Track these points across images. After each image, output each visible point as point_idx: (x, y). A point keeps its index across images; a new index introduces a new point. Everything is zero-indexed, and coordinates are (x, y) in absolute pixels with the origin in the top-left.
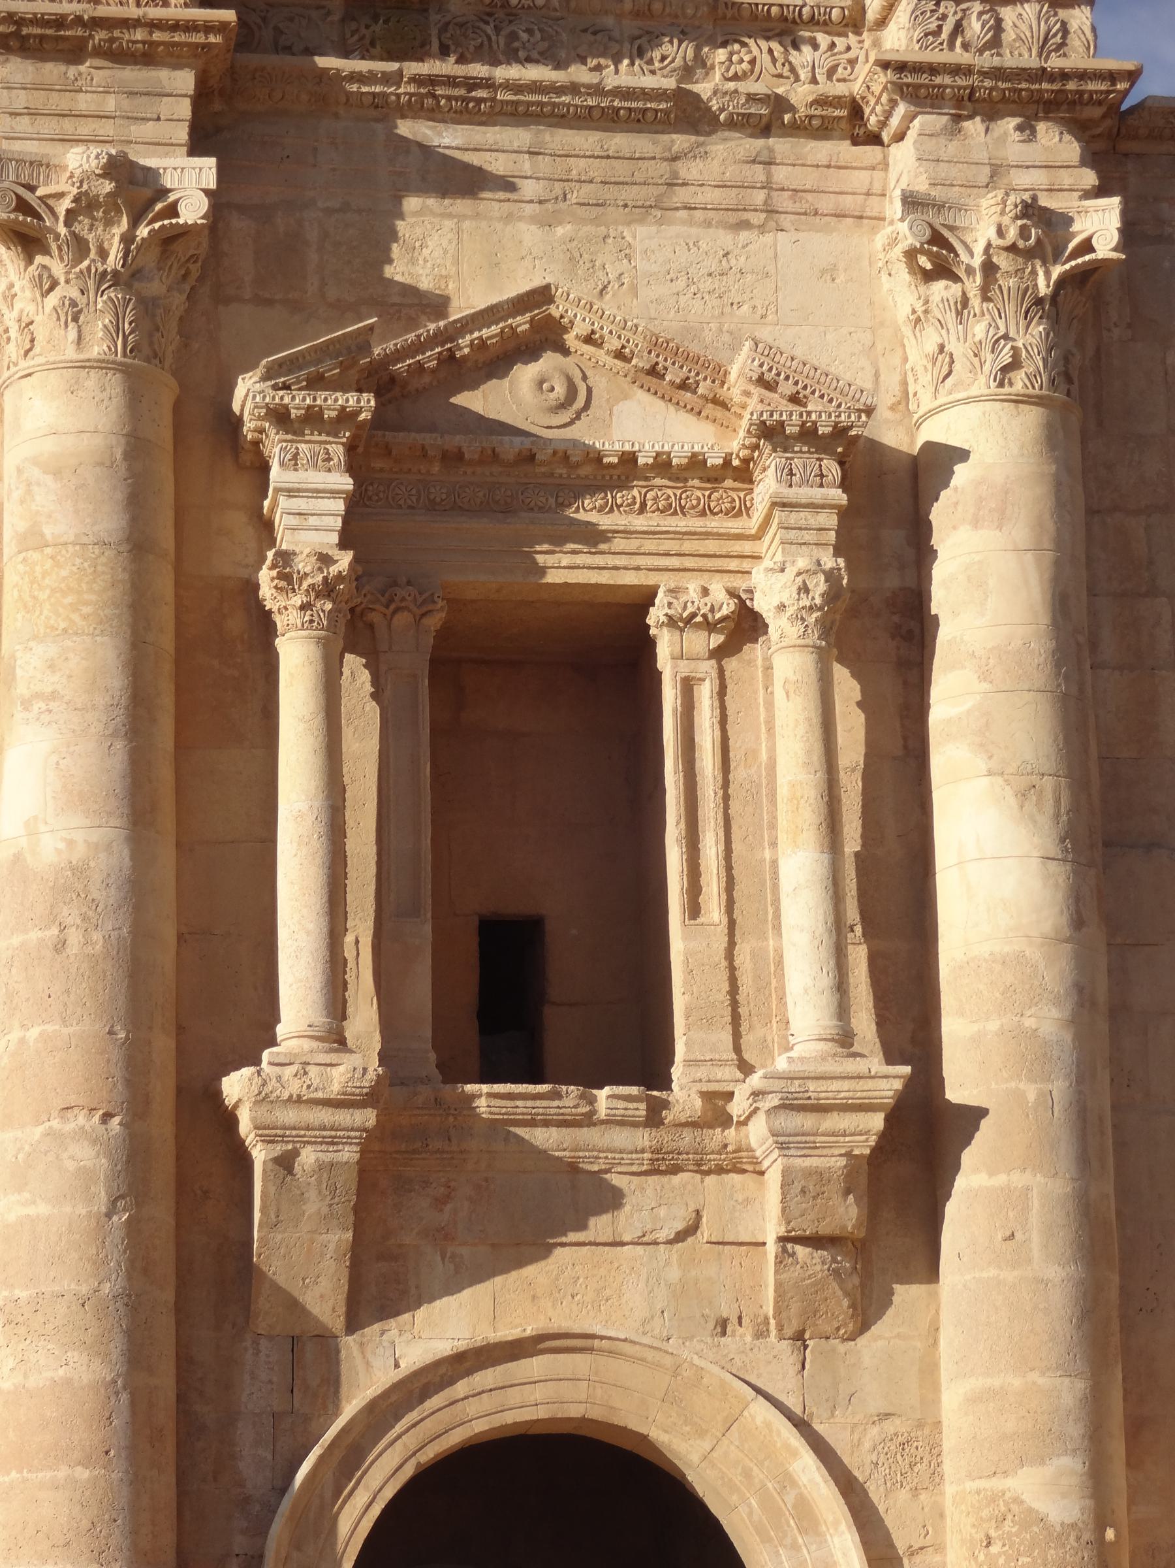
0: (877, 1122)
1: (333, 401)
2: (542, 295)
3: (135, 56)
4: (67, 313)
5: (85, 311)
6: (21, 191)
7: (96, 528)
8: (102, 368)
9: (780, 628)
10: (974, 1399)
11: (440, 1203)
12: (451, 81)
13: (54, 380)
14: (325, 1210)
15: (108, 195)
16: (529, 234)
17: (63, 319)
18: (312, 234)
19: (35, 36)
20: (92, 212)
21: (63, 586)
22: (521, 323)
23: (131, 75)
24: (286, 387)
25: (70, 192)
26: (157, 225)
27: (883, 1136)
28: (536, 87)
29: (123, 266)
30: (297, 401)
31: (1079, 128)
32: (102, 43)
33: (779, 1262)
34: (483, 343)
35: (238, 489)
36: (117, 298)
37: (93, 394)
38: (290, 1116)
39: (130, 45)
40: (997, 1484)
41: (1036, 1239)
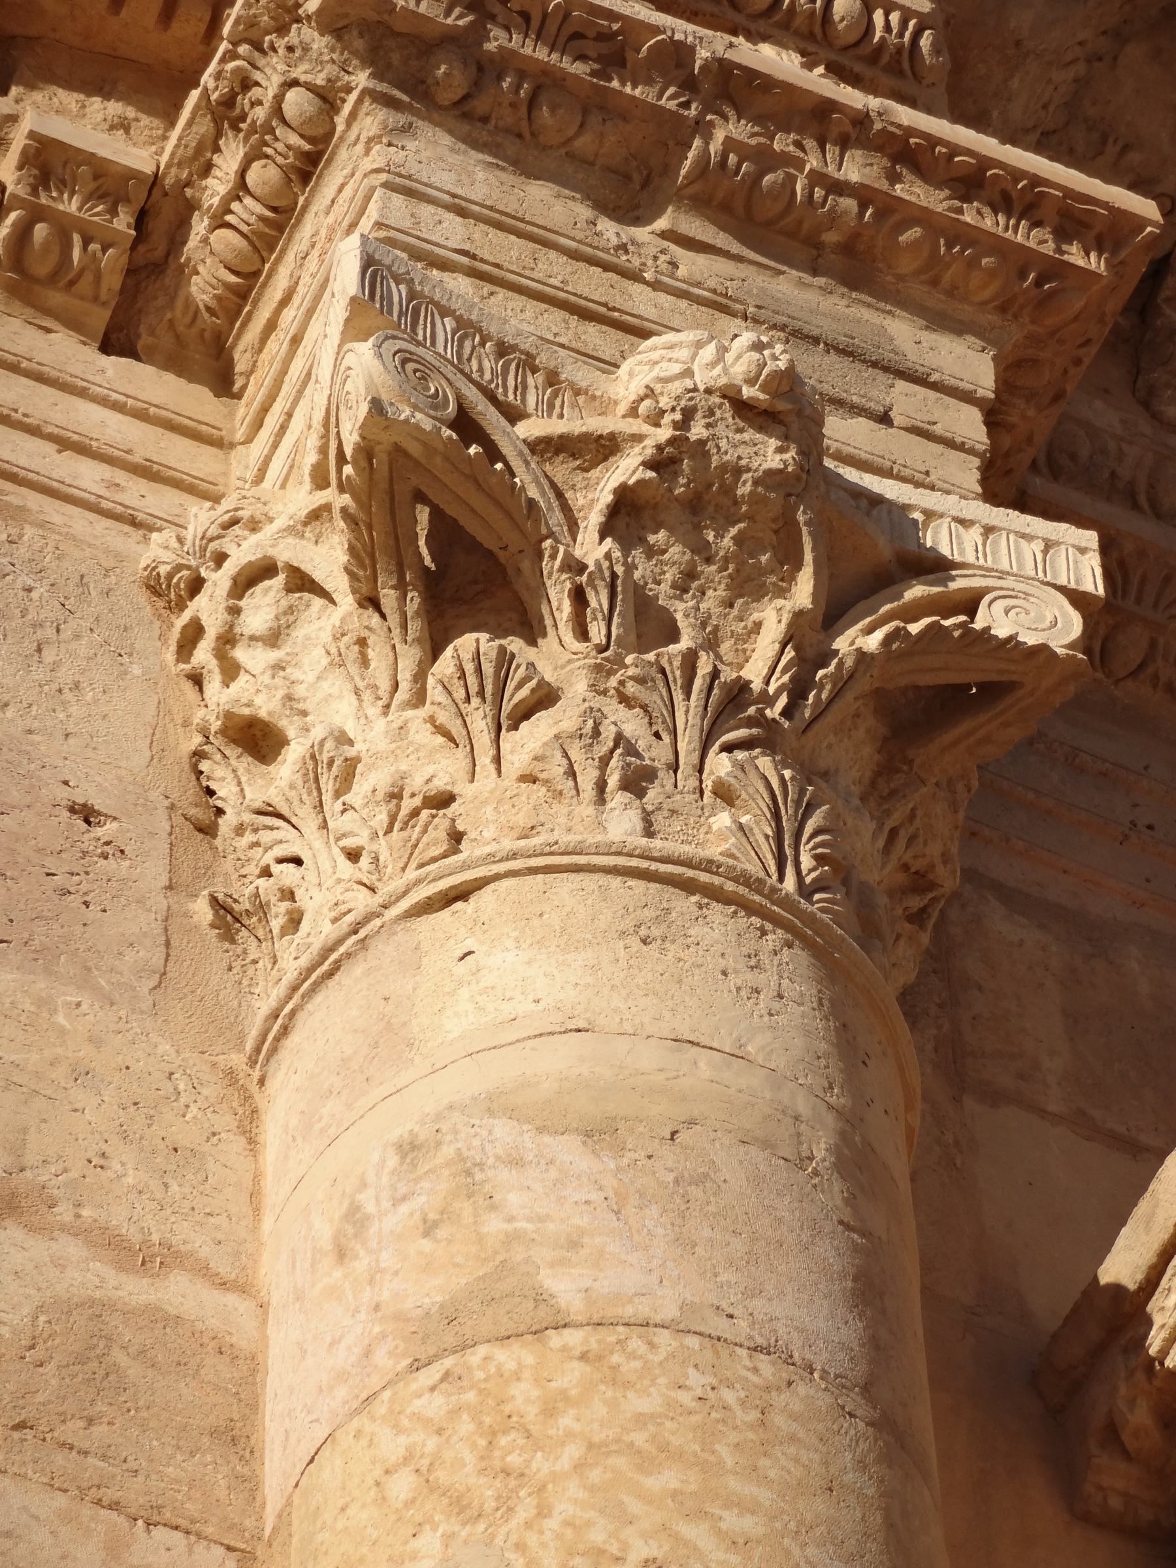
3: (819, 246)
4: (605, 761)
5: (663, 775)
6: (472, 394)
7: (758, 1304)
8: (751, 909)
15: (770, 478)
17: (587, 778)
19: (523, 69)
20: (698, 528)
21: (639, 1439)
25: (638, 438)
29: (787, 713)
32: (732, 159)
36: (782, 778)
37: (722, 963)
39: (818, 193)
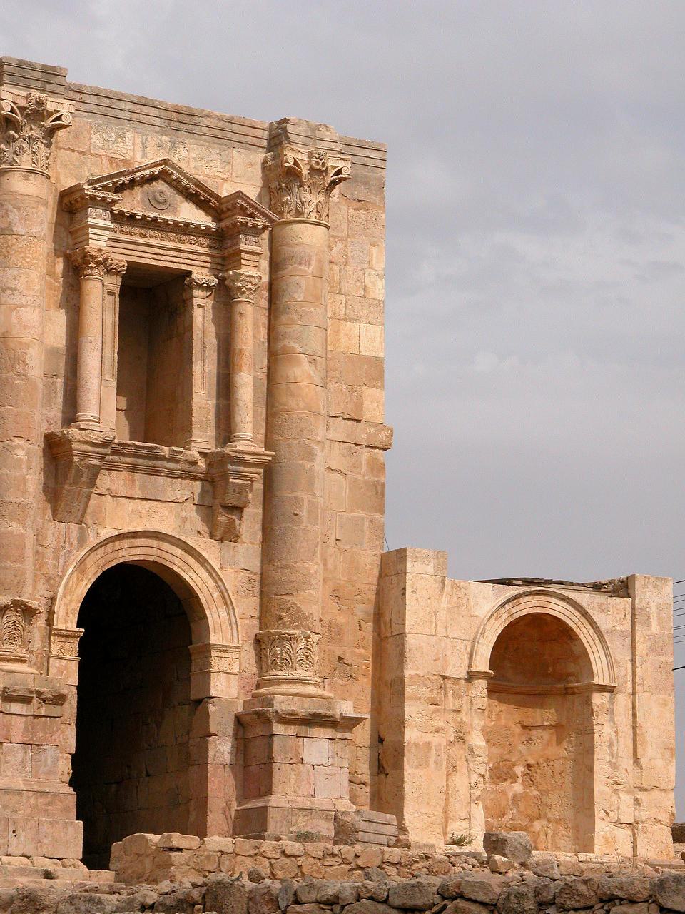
2: (165, 162)
14: (88, 481)
22: (156, 170)
24: (95, 189)
26: (53, 123)
30: (100, 194)
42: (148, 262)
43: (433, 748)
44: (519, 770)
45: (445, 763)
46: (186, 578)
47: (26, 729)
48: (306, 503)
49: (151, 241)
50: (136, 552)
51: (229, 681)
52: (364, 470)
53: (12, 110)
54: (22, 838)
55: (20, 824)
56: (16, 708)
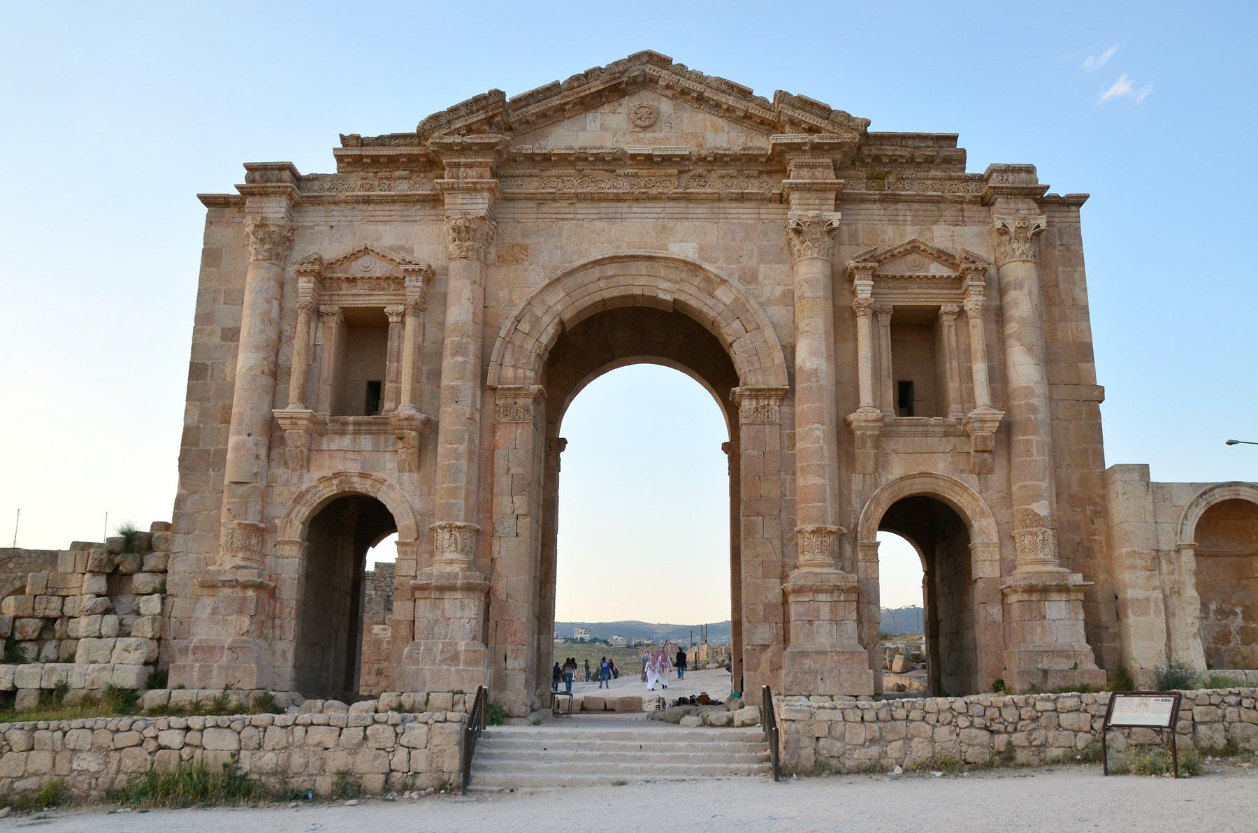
0: (998, 424)
1: (869, 264)
2: (914, 241)
9: (970, 313)
10: (1021, 487)
11: (896, 444)
12: (891, 194)
13: (806, 262)
16: (909, 228)
18: (860, 229)
23: (821, 195)
27: (999, 428)
28: (910, 195)
30: (860, 265)
31: (1036, 200)
33: (975, 457)
34: (900, 253)
35: (847, 285)
38: (863, 424)
40: (1028, 507)
41: (1034, 450)
42: (909, 304)
43: (1152, 599)
44: (1238, 610)
45: (1163, 611)
46: (955, 501)
47: (831, 610)
48: (1034, 443)
49: (910, 291)
50: (916, 487)
51: (992, 565)
52: (1084, 417)
53: (798, 224)
54: (828, 683)
55: (826, 674)
56: (822, 597)
